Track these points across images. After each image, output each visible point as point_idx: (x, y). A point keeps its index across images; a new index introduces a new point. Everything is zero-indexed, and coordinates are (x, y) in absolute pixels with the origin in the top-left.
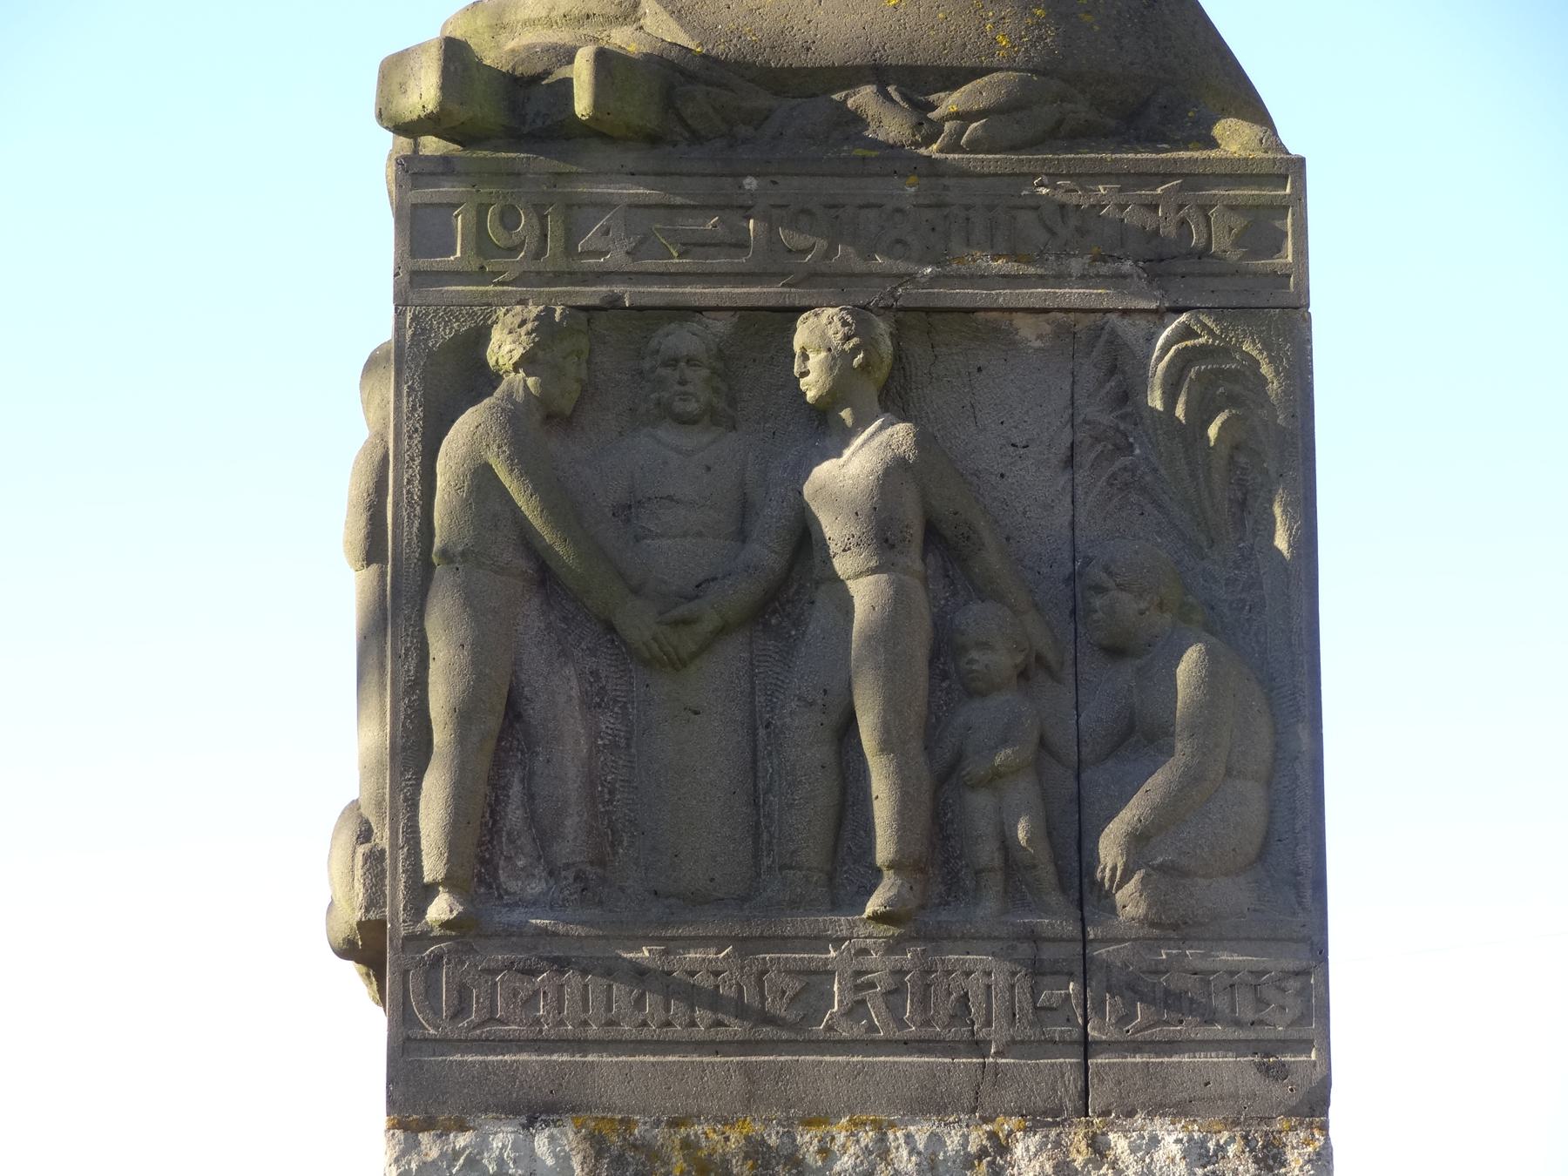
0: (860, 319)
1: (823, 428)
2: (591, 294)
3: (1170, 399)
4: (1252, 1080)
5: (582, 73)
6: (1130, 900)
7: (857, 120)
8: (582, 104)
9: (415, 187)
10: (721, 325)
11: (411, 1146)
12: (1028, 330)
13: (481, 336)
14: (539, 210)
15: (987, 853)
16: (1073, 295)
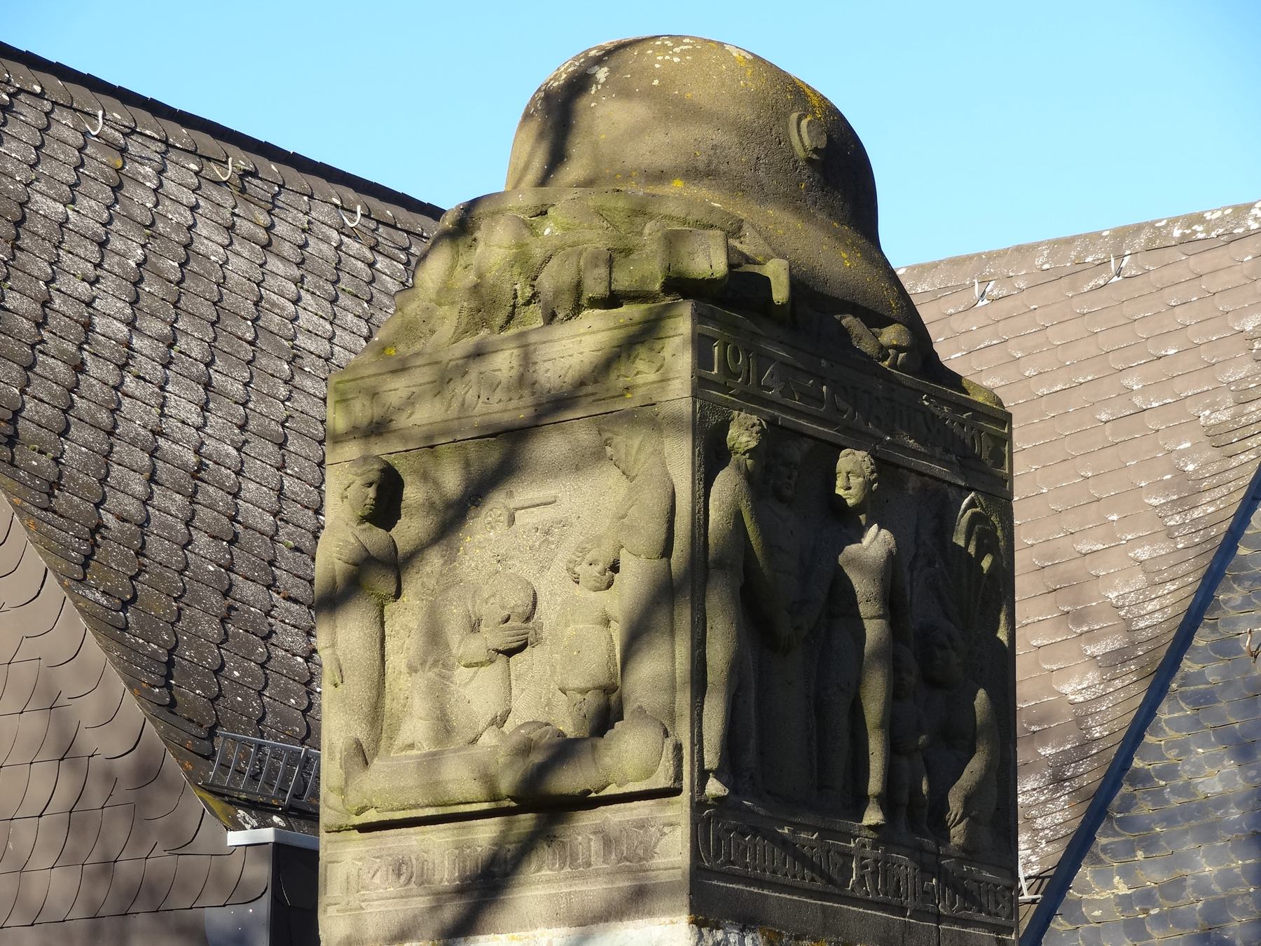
0: (881, 464)
1: (847, 523)
3: (967, 544)
6: (957, 834)
7: (845, 333)
8: (780, 294)
9: (700, 323)
12: (913, 483)
13: (724, 427)
14: (747, 352)
15: (904, 796)
16: (937, 469)
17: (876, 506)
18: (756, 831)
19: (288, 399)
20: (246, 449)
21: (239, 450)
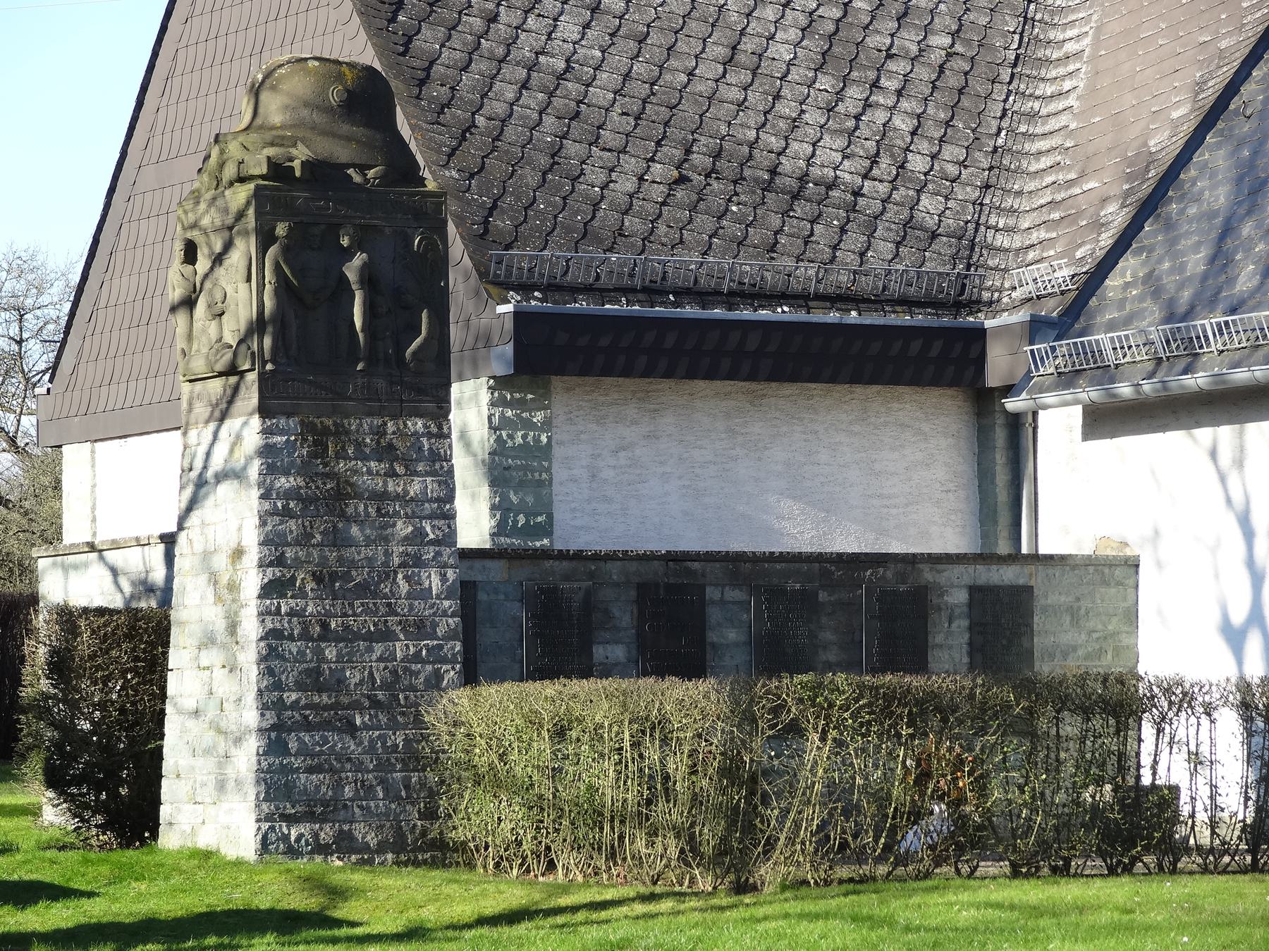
1: (348, 254)
2: (297, 220)
4: (435, 410)
5: (296, 164)
7: (349, 176)
8: (298, 174)
10: (323, 227)
11: (264, 422)
17: (358, 245)
18: (293, 380)
19: (661, 5)
20: (610, 50)
21: (603, 52)
